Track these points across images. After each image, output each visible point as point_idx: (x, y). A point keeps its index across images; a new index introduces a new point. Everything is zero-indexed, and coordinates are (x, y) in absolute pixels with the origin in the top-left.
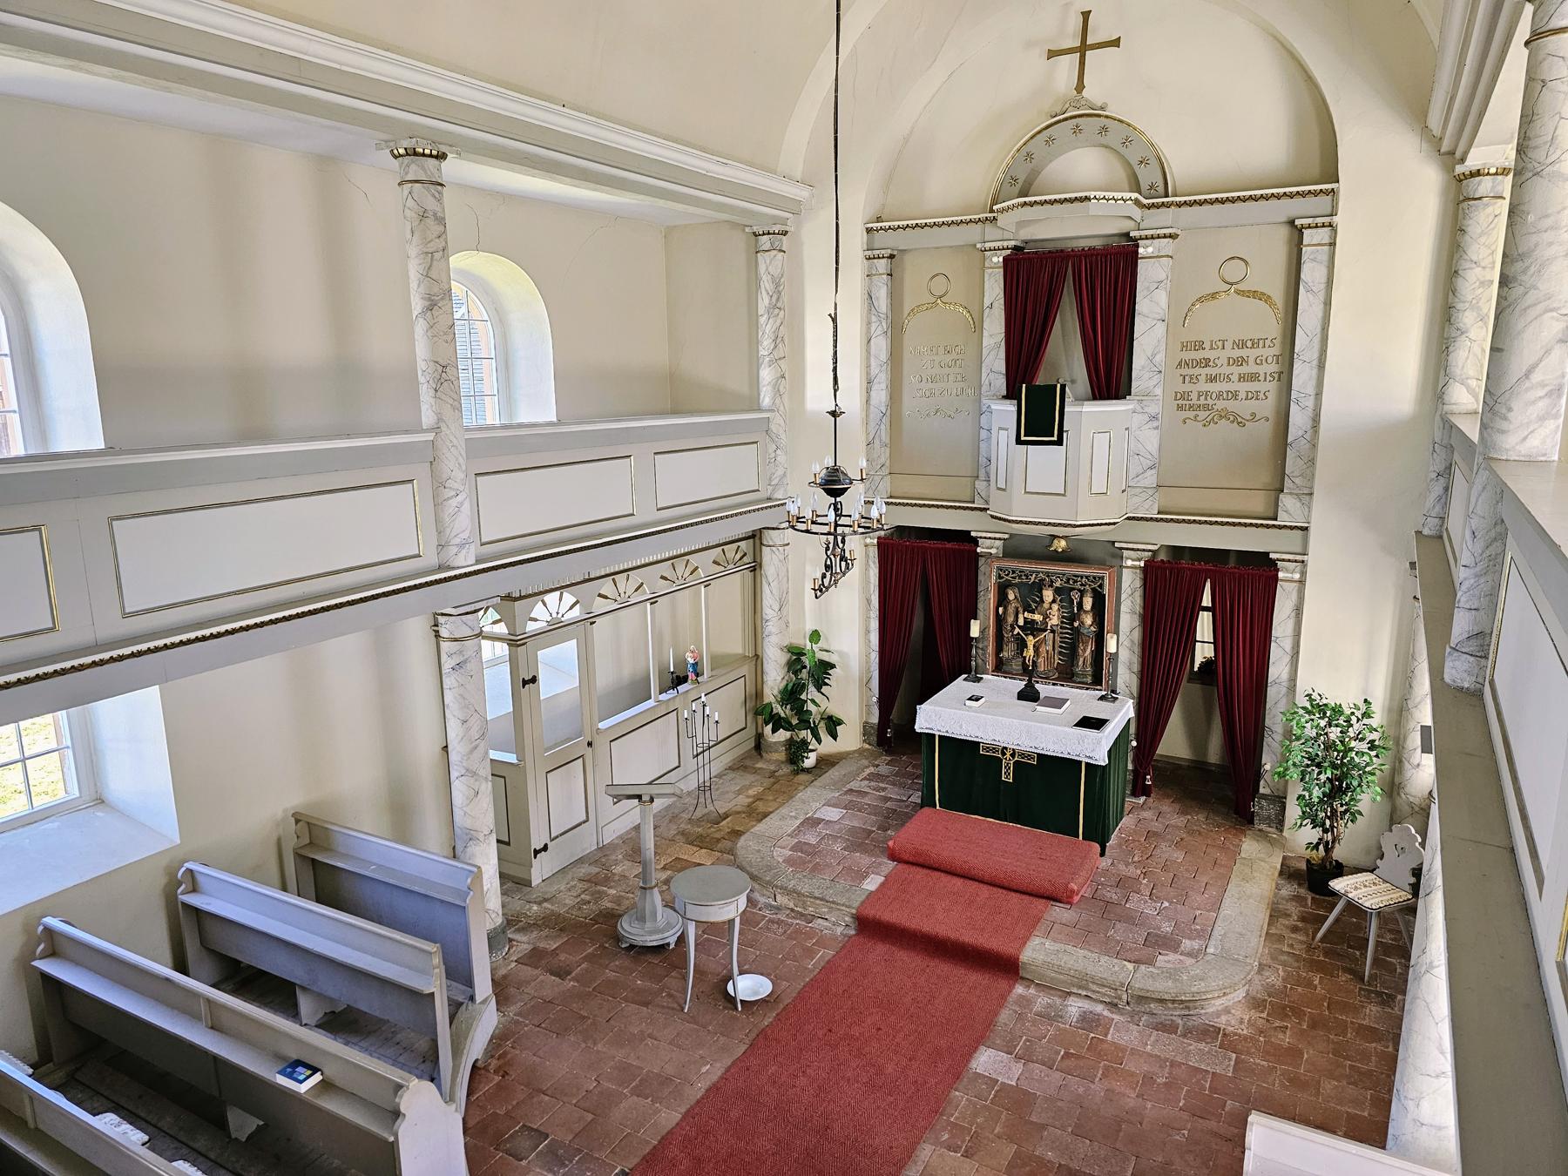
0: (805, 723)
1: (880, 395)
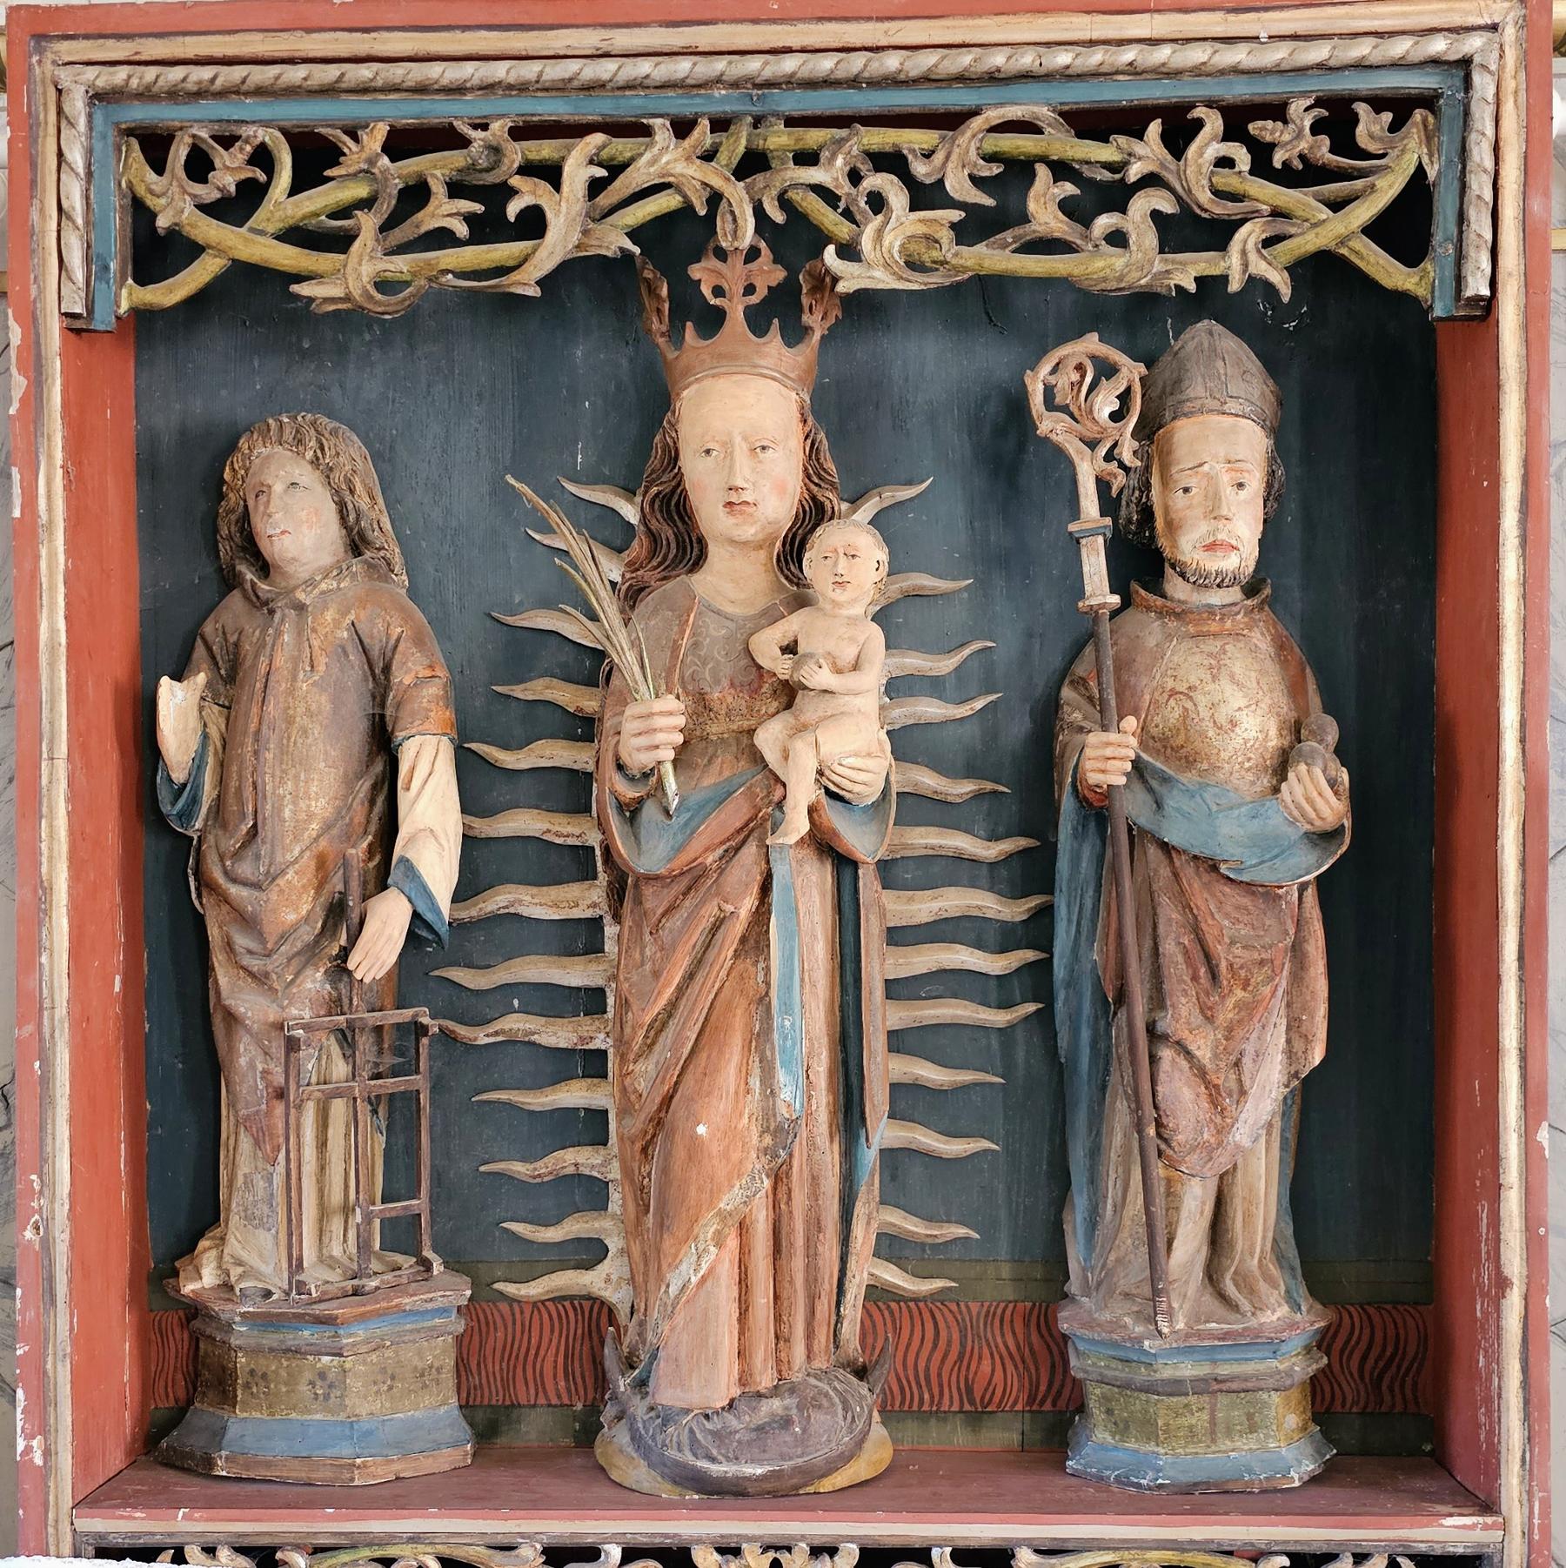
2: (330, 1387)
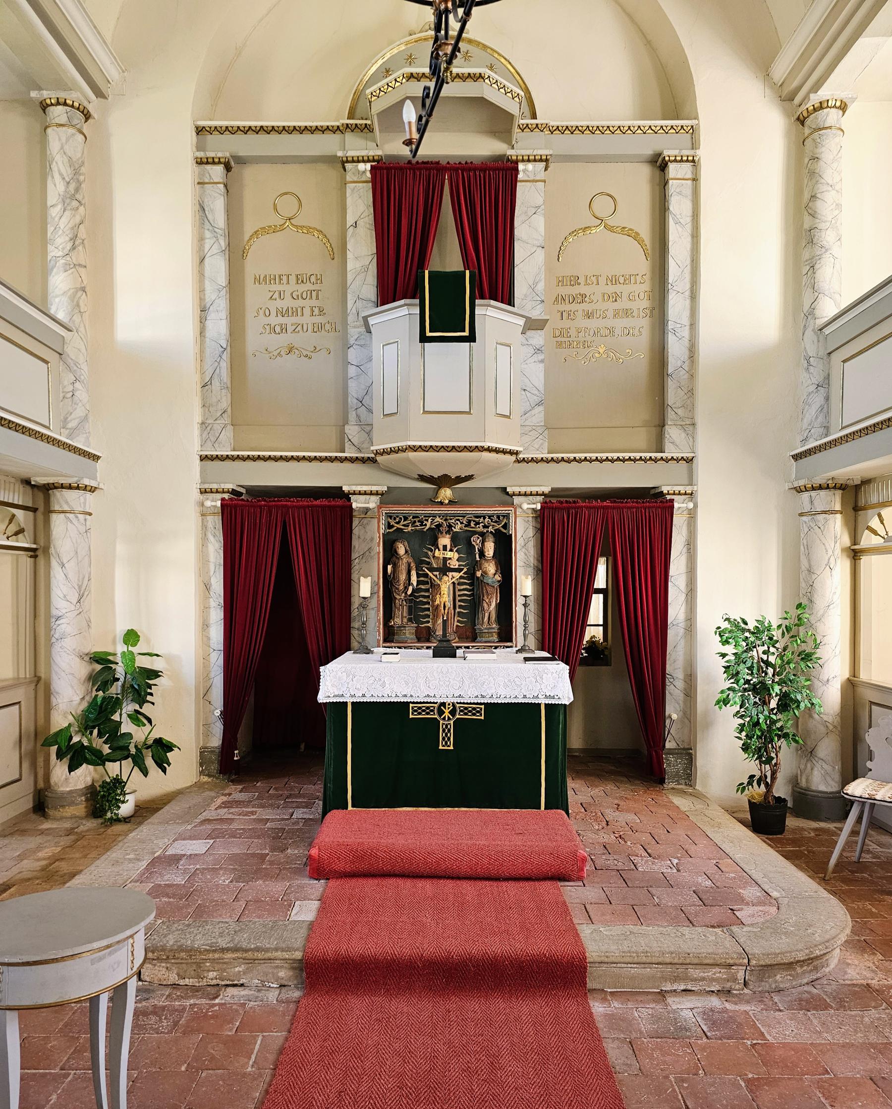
0: (121, 748)
1: (218, 326)
2: (405, 634)
